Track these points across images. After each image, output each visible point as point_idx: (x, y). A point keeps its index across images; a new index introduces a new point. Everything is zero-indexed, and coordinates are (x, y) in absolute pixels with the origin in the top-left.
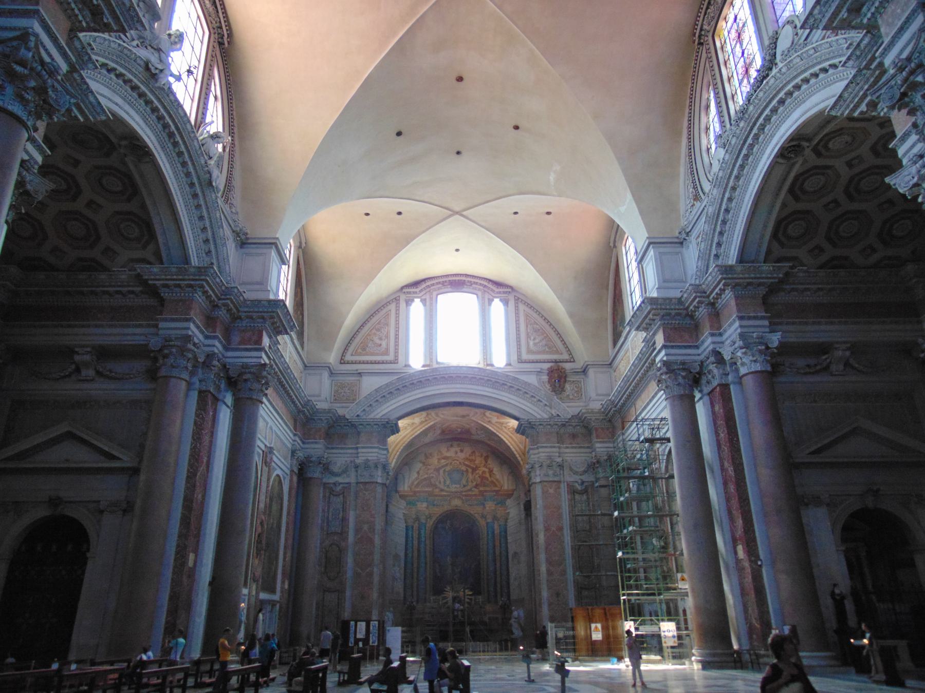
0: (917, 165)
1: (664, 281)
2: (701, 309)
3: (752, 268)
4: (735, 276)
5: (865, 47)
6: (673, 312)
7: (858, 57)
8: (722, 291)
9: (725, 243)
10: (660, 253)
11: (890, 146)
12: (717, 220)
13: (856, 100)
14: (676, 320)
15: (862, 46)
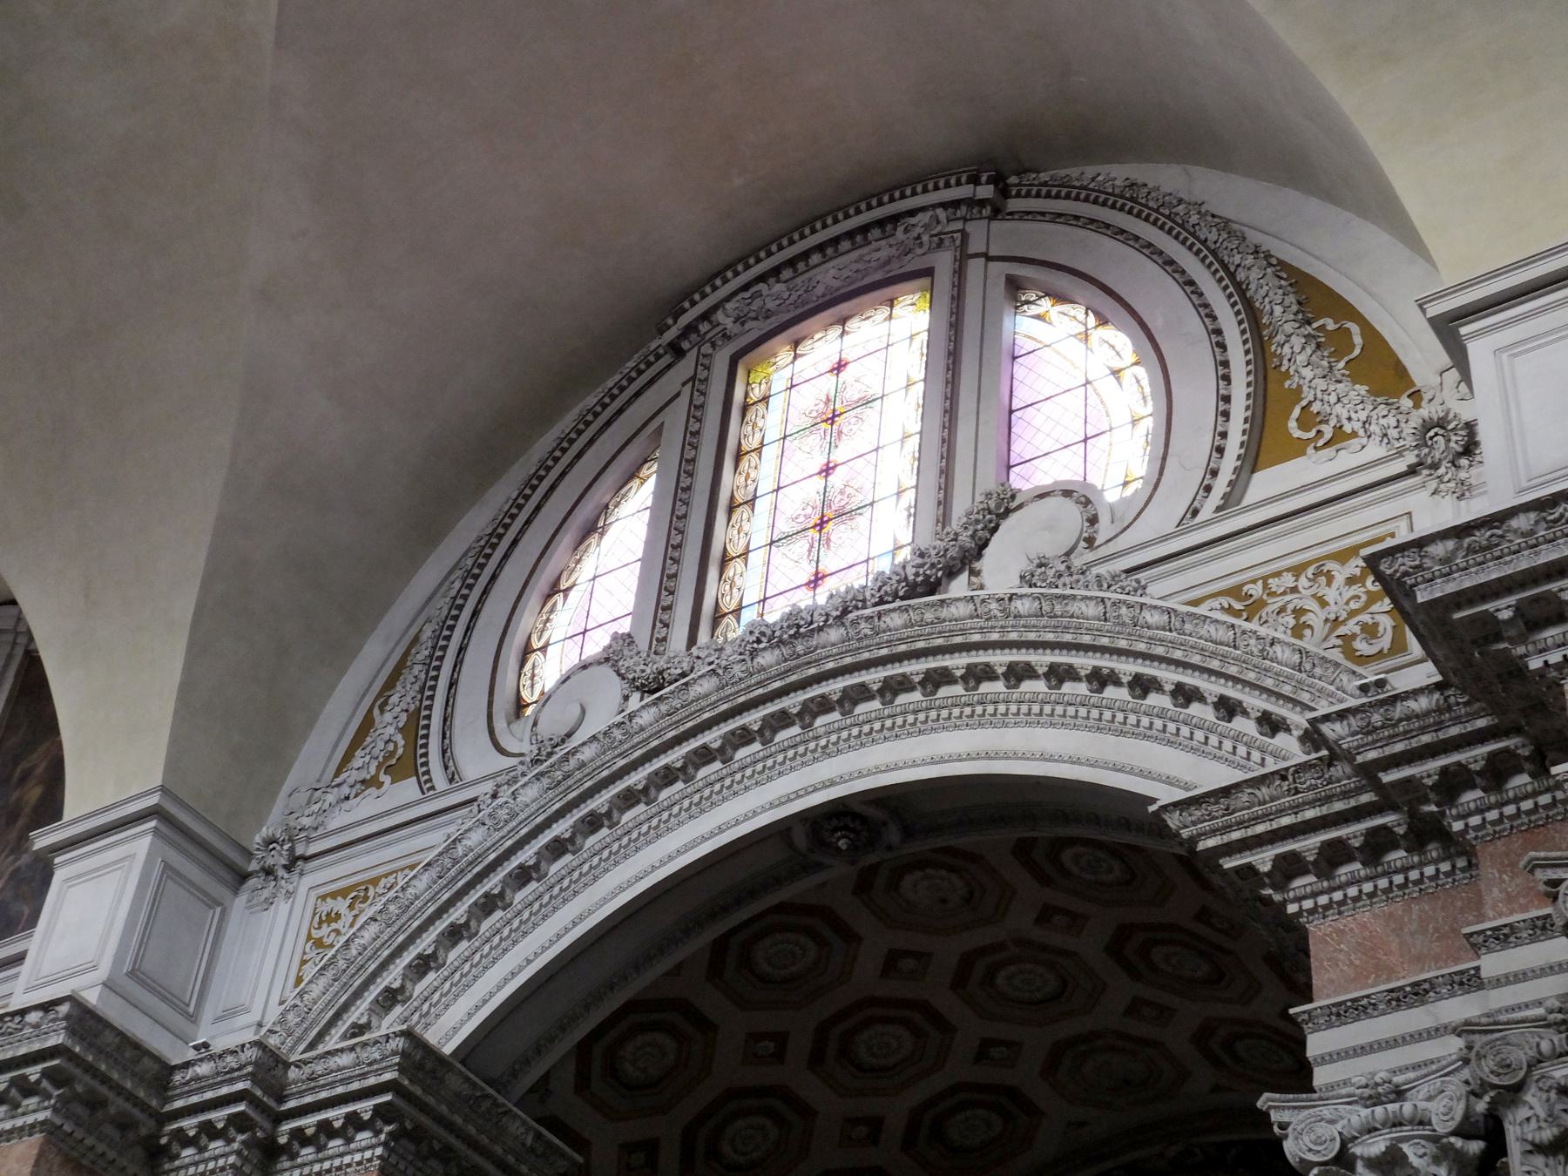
0: (1379, 1110)
1: (133, 974)
2: (217, 1146)
3: (486, 1104)
4: (431, 1100)
5: (1408, 718)
6: (117, 1104)
7: (1369, 730)
8: (354, 1123)
9: (444, 972)
10: (167, 867)
11: (1292, 1011)
12: (470, 886)
13: (1260, 829)
14: (100, 1139)
15: (1399, 710)
